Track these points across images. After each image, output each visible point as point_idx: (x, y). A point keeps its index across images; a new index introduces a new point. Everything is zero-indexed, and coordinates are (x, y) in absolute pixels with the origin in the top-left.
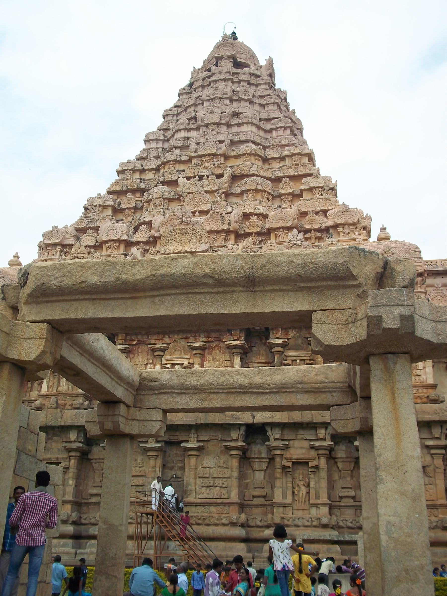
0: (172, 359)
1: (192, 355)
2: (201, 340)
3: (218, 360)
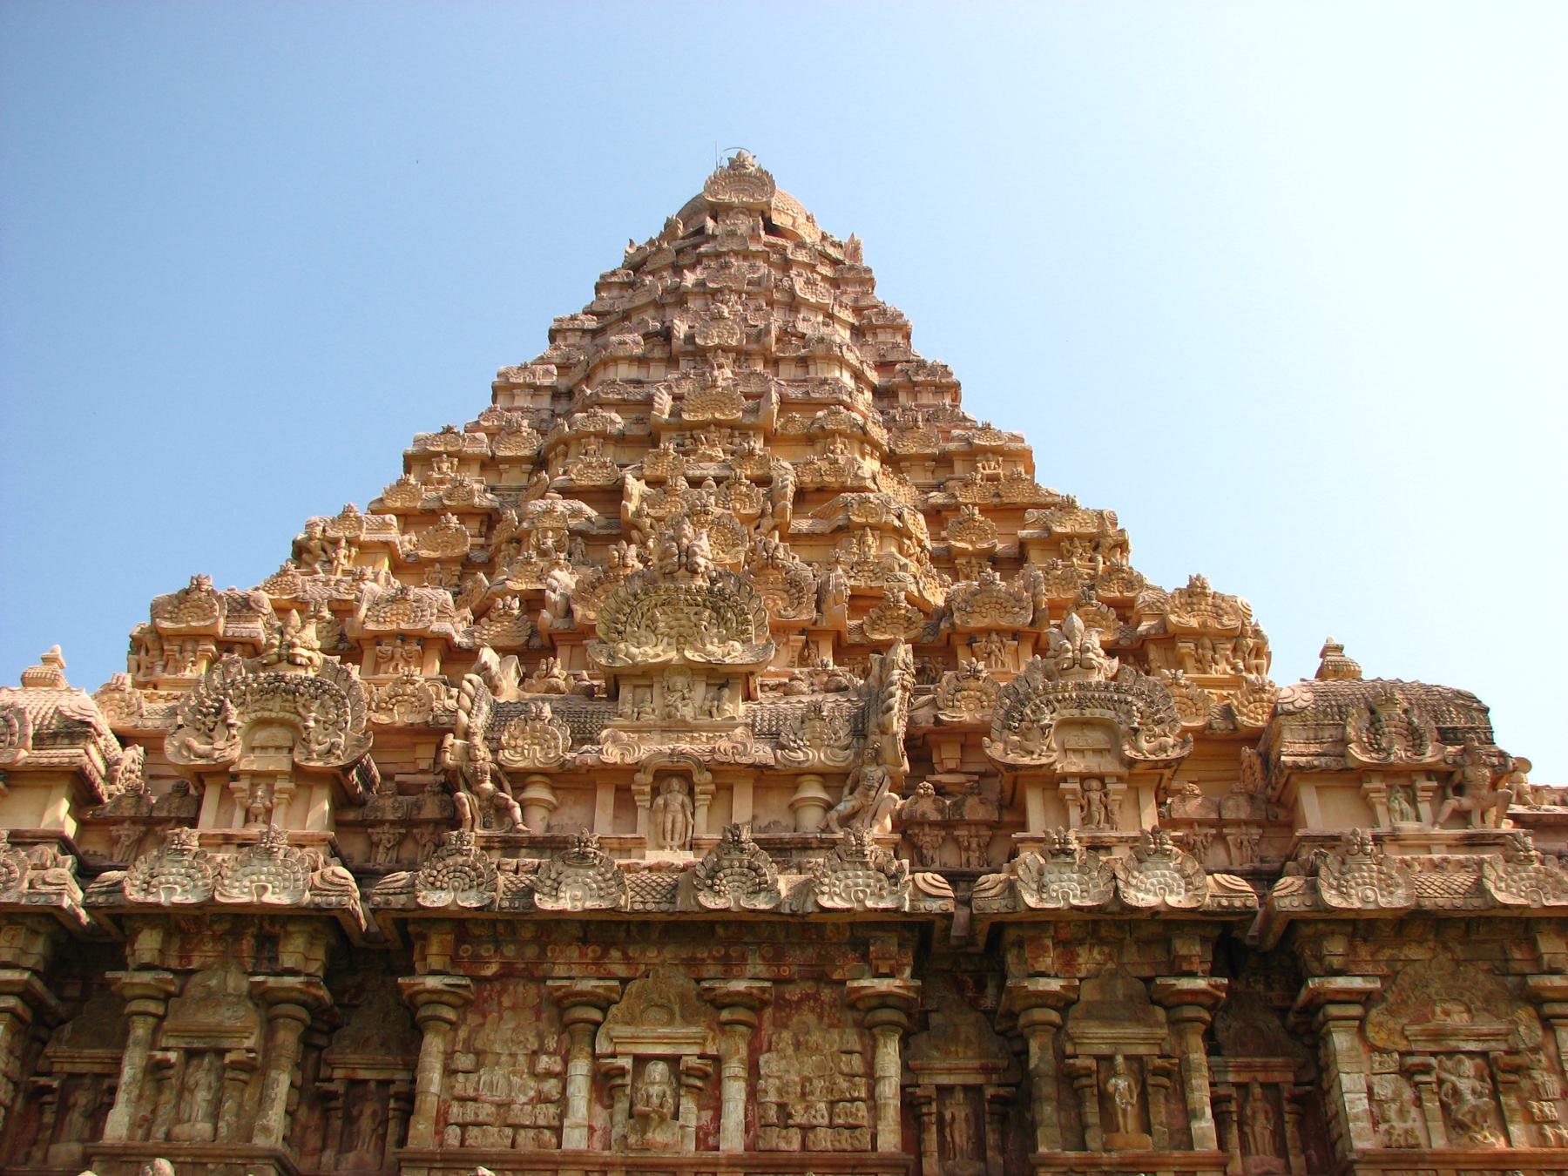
0: (635, 1040)
1: (715, 1026)
2: (750, 970)
3: (817, 1049)
